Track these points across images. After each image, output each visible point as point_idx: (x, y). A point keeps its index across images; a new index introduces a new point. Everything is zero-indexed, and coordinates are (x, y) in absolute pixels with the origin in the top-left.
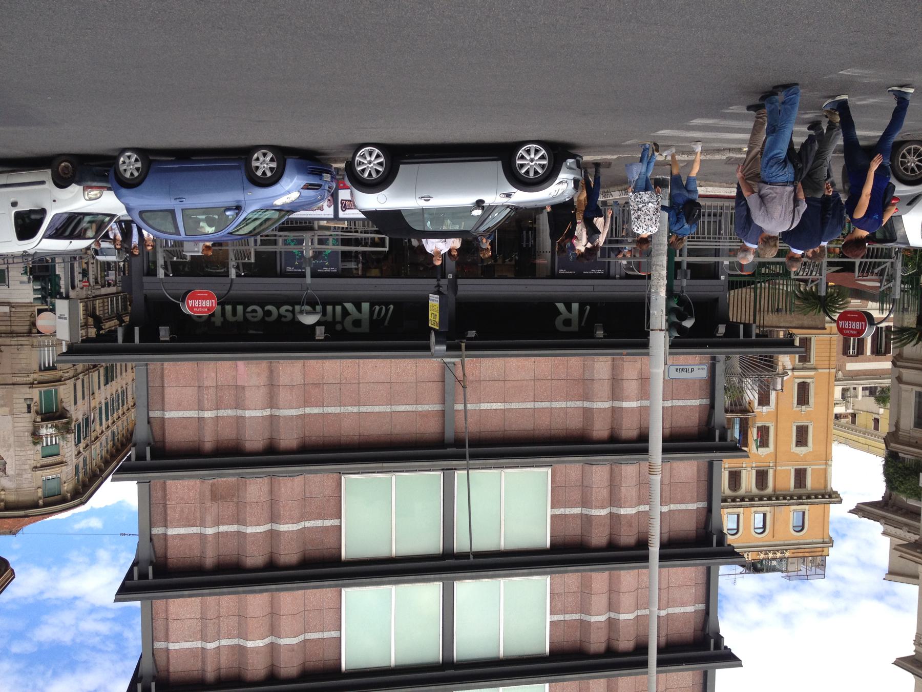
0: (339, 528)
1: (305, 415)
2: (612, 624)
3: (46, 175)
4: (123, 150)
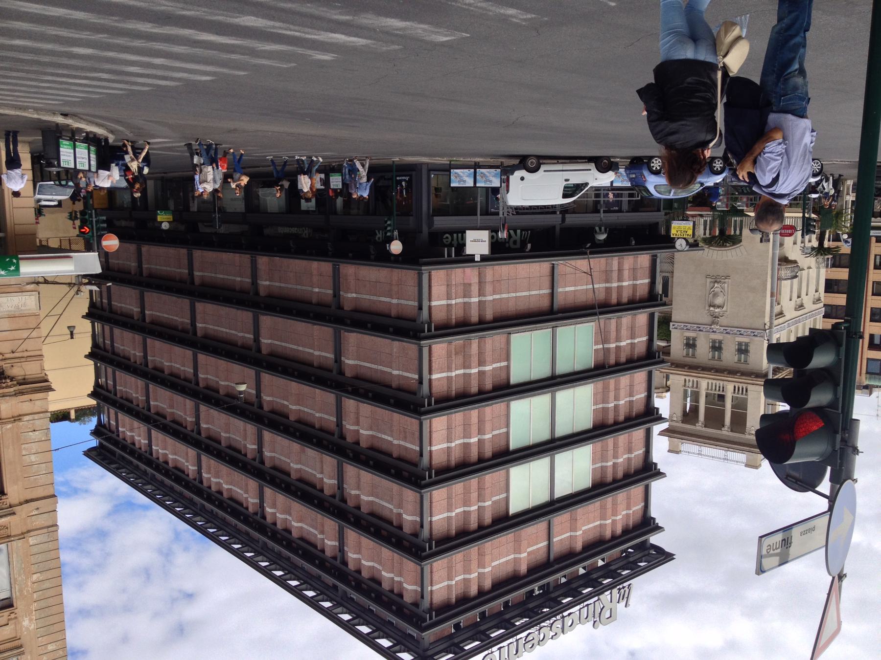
0: (508, 367)
2: (616, 407)
3: (592, 166)
4: (653, 157)
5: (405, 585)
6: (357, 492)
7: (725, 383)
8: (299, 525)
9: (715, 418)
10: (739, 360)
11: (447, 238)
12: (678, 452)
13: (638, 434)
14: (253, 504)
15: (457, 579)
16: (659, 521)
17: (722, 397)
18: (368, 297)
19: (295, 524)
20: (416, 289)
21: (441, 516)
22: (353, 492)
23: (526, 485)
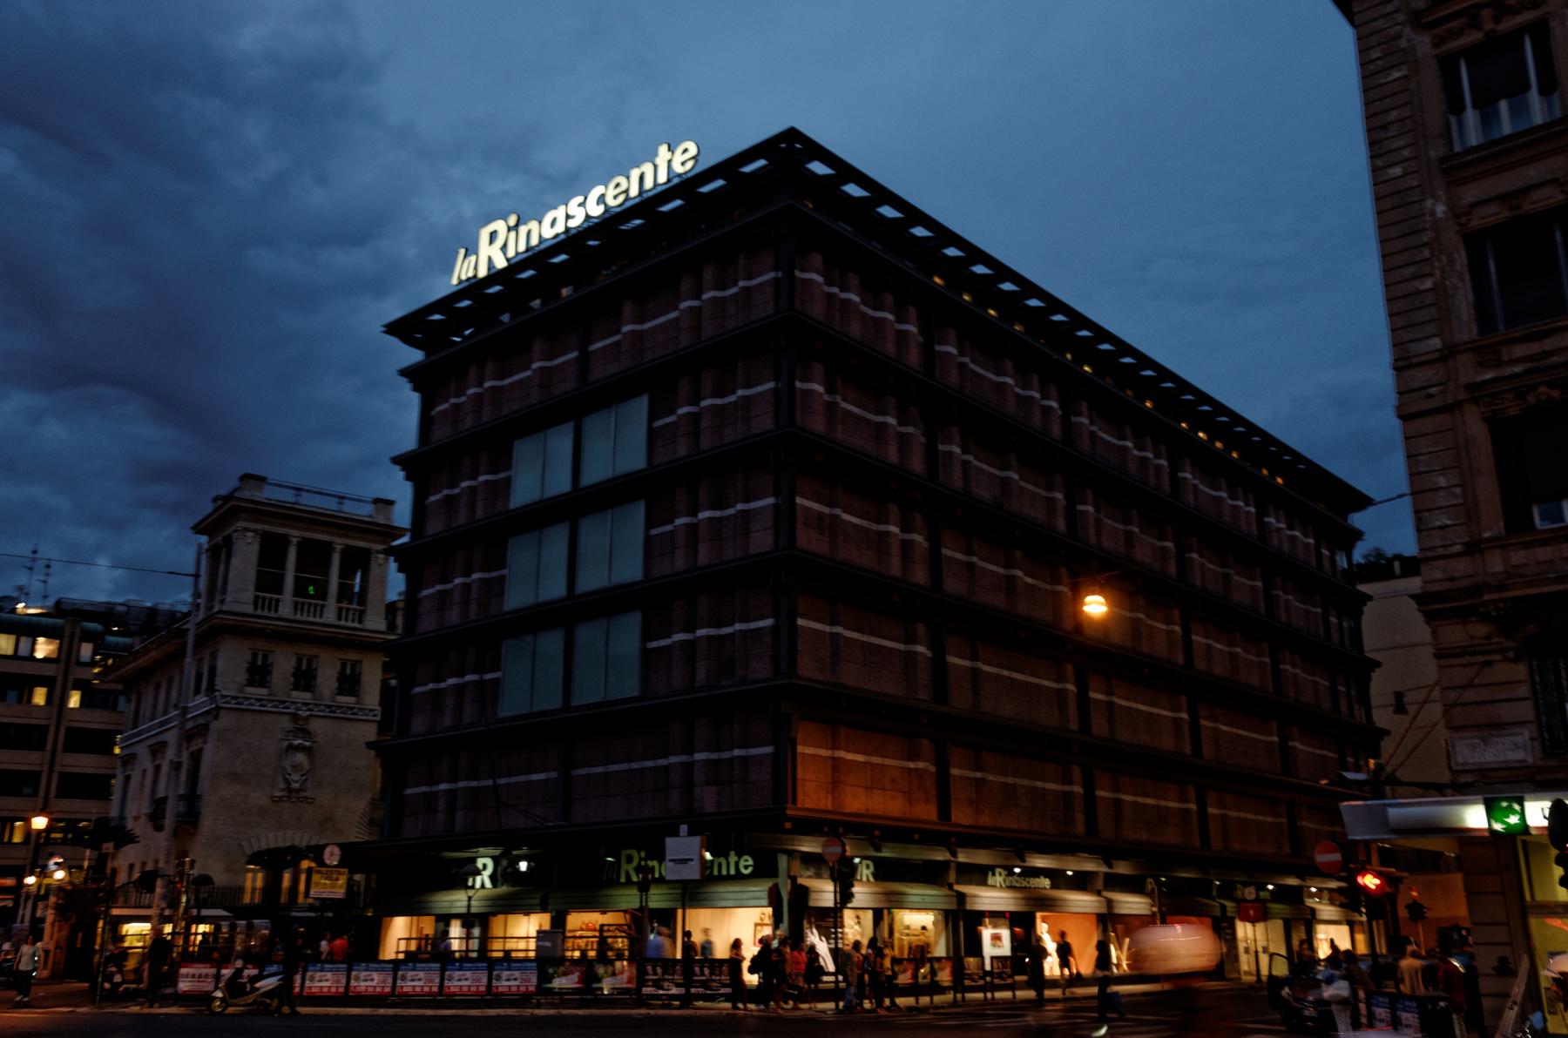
1: (666, 757)
5: (820, 279)
6: (903, 429)
7: (291, 617)
8: (1001, 379)
9: (315, 557)
10: (265, 657)
11: (746, 867)
12: (377, 501)
13: (435, 527)
14: (1080, 414)
15: (734, 290)
16: (405, 387)
17: (300, 590)
18: (888, 762)
19: (1008, 380)
20: (799, 776)
21: (760, 389)
22: (910, 430)
23: (620, 444)
